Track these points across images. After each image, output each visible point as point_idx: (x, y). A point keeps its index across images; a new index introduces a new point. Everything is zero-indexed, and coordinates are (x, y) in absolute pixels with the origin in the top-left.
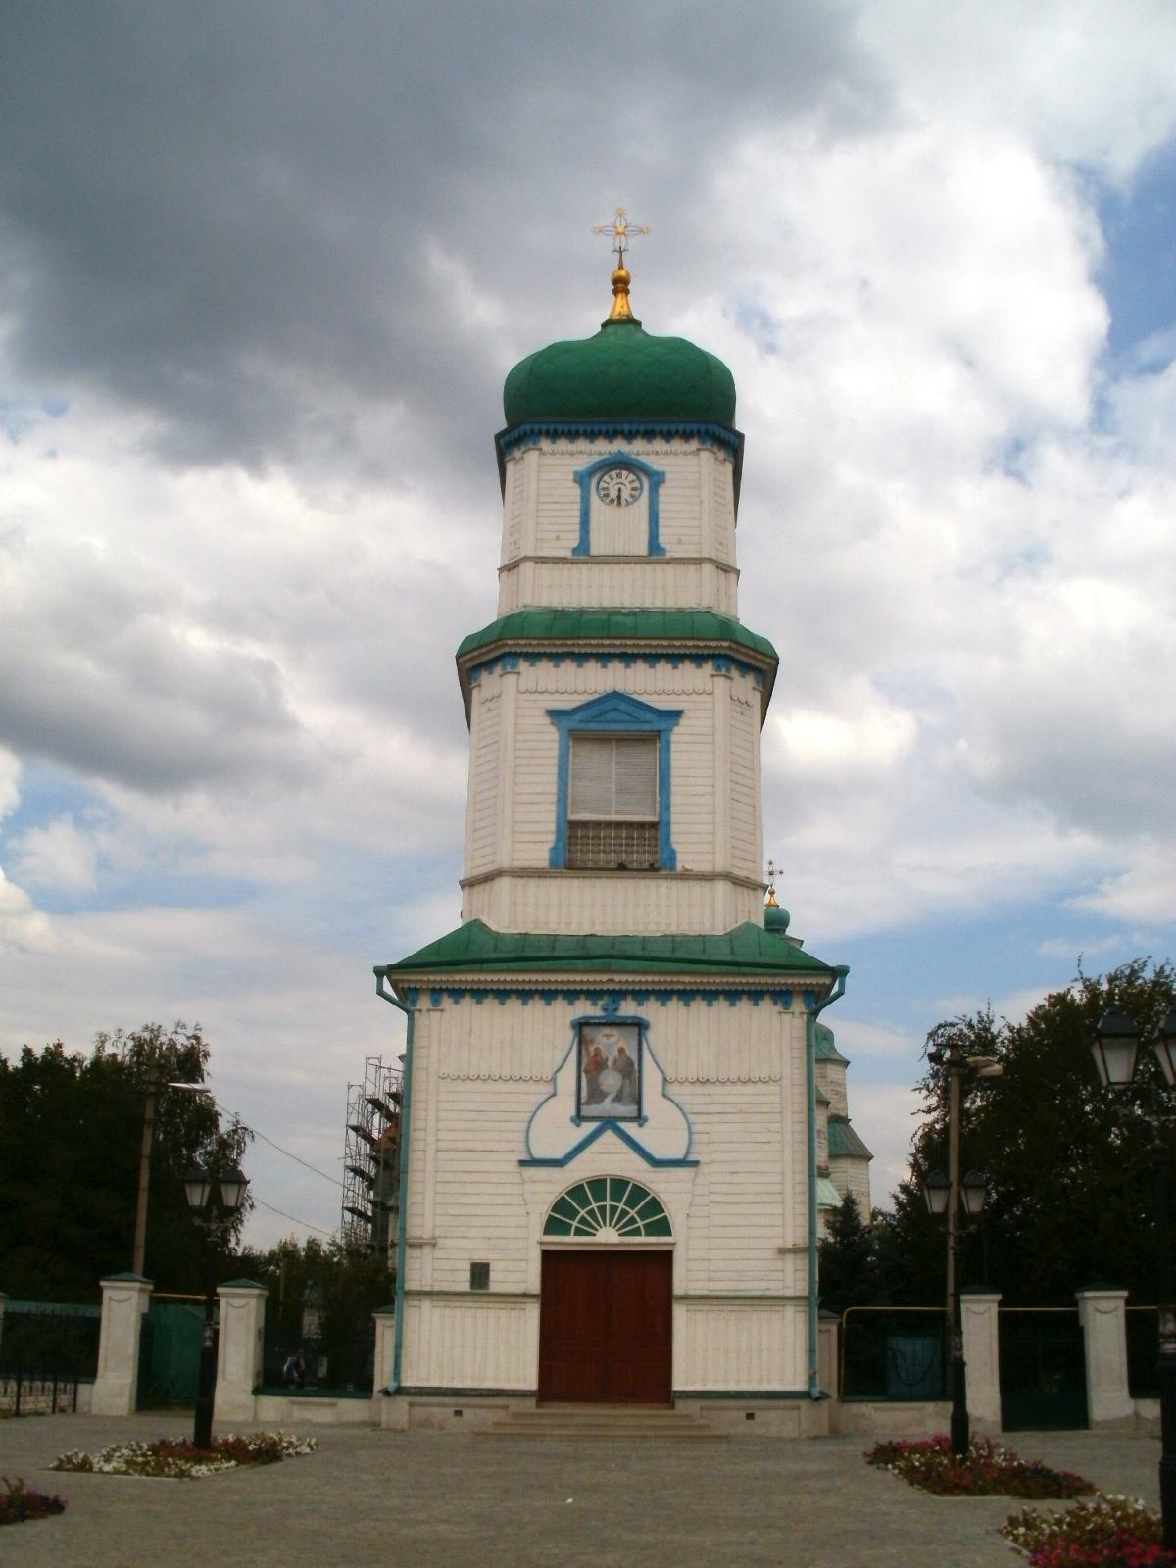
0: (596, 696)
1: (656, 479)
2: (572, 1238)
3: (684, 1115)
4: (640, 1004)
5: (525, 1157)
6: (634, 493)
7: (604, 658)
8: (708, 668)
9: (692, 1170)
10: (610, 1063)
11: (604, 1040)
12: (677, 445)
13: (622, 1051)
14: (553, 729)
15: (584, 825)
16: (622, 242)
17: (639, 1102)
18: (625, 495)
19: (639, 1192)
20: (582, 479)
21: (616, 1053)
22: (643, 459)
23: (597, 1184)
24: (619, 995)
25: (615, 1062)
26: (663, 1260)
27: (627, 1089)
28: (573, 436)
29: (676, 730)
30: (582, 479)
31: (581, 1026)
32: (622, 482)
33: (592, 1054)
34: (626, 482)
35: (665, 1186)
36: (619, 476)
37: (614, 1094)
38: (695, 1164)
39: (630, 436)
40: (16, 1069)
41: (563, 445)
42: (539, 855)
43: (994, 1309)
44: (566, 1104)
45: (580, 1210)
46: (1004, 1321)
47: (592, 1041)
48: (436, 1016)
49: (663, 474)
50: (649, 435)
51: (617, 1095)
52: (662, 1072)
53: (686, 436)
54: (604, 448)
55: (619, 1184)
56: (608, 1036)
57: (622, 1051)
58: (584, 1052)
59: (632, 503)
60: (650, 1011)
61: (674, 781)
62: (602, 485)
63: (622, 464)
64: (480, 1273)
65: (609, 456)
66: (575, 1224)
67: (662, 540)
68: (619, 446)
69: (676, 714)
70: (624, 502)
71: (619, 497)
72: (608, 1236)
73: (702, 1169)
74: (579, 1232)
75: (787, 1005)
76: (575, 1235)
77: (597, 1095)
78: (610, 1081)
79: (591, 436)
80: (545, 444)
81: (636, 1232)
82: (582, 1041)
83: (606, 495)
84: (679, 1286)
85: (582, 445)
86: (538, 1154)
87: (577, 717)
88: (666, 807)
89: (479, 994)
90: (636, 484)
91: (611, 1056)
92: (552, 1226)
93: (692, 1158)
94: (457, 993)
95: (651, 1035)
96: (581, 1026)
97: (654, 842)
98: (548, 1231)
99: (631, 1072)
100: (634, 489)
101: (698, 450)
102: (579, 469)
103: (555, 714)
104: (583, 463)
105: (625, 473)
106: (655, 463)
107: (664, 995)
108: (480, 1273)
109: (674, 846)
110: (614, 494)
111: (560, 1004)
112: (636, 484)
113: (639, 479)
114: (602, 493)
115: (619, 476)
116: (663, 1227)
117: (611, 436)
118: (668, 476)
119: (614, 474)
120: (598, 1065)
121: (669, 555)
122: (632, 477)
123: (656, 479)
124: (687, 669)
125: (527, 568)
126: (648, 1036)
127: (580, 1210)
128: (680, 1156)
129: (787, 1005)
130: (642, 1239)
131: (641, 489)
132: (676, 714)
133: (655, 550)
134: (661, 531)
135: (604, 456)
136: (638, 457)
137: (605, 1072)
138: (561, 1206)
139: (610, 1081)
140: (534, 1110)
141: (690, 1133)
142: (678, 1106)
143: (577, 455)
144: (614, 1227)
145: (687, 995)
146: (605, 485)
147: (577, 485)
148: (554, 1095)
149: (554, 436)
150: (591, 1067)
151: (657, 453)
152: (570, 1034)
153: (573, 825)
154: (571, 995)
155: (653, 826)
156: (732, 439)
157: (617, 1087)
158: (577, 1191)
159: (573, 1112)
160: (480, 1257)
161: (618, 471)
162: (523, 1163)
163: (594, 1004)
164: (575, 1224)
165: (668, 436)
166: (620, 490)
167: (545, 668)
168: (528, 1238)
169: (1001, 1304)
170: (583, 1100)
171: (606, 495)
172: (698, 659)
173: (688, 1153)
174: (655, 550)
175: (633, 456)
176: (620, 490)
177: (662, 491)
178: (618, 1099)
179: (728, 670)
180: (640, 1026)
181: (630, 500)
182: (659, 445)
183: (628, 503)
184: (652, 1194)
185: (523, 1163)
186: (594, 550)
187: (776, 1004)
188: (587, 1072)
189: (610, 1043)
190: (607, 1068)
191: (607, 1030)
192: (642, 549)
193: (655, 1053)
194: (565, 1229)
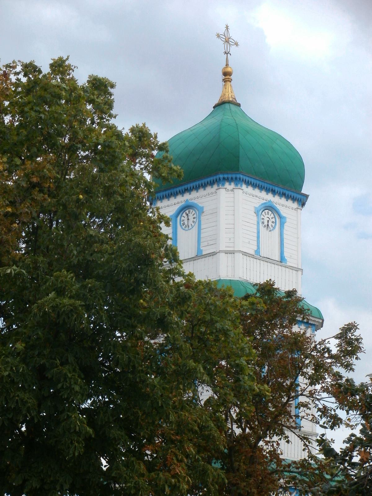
6: (273, 225)
12: (290, 203)
18: (270, 223)
22: (279, 207)
32: (268, 216)
41: (250, 190)
49: (285, 218)
50: (282, 195)
53: (294, 199)
59: (273, 230)
63: (270, 208)
65: (266, 202)
67: (286, 254)
68: (270, 197)
71: (268, 225)
79: (261, 188)
80: (244, 186)
85: (257, 192)
100: (273, 222)
101: (298, 208)
105: (270, 212)
106: (283, 211)
110: (266, 223)
112: (274, 220)
117: (268, 190)
118: (288, 220)
119: (266, 211)
121: (289, 264)
122: (272, 216)
131: (275, 223)
133: (282, 259)
134: (285, 250)
136: (275, 205)
149: (248, 183)
151: (283, 206)
161: (268, 211)
165: (288, 197)
171: (263, 223)
175: (274, 204)
181: (271, 228)
182: (283, 201)
186: (263, 253)
192: (277, 258)
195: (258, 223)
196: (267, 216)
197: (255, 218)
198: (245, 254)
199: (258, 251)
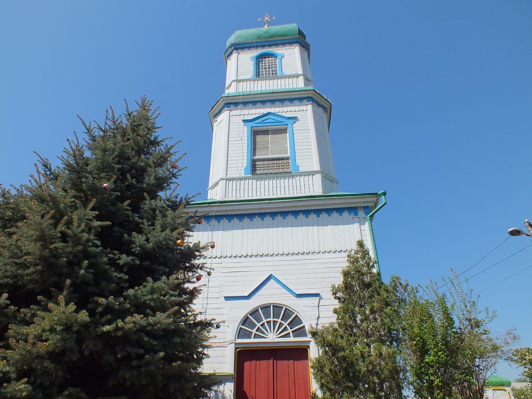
0: (261, 115)
2: (252, 340)
19: (288, 313)
23: (265, 308)
40: (76, 306)
55: (277, 308)
74: (256, 336)
75: (356, 214)
76: (254, 338)
81: (287, 335)
92: (241, 333)
103: (245, 121)
129: (356, 214)
130: (292, 339)
138: (245, 321)
158: (254, 313)
164: (254, 331)
184: (296, 313)
187: (350, 214)
194: (248, 335)
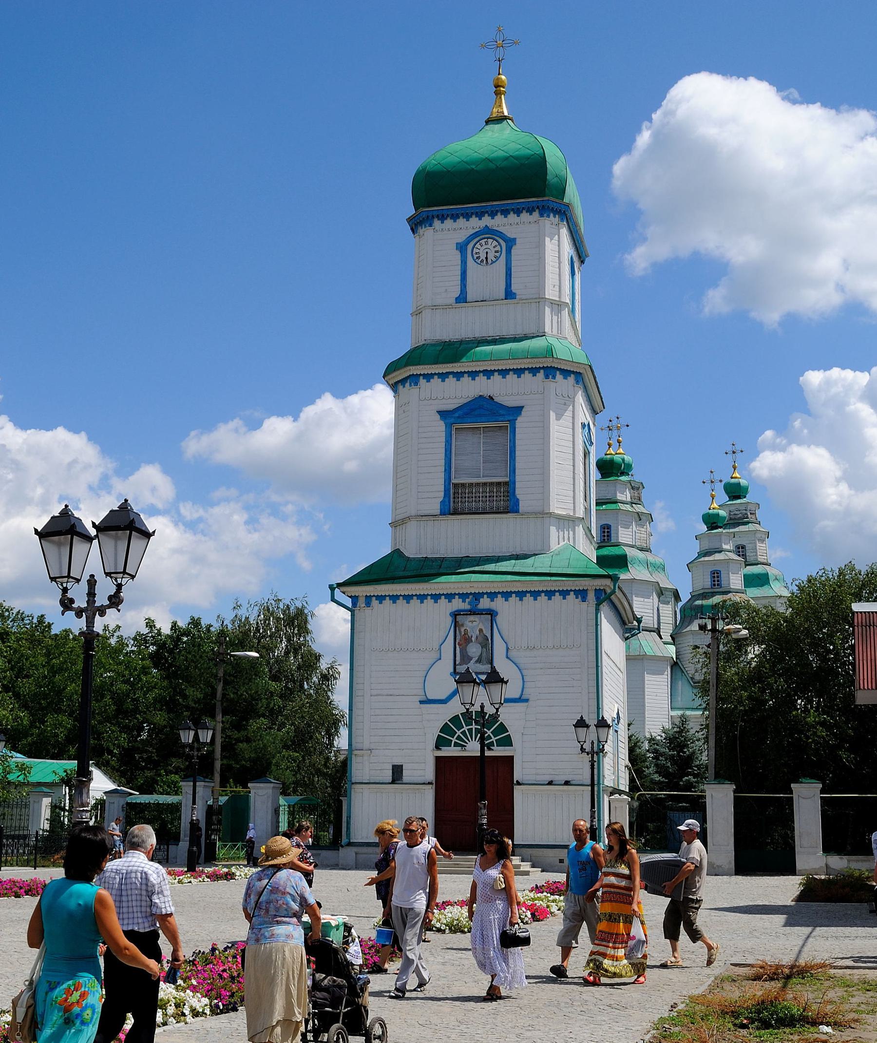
1: (510, 243)
3: (520, 670)
4: (492, 600)
5: (424, 698)
6: (496, 254)
7: (473, 374)
8: (541, 375)
9: (526, 704)
10: (473, 639)
11: (470, 624)
12: (525, 216)
13: (481, 631)
14: (442, 423)
15: (463, 485)
16: (500, 53)
17: (491, 663)
18: (491, 257)
20: (462, 248)
21: (478, 632)
22: (500, 229)
24: (477, 596)
25: (477, 637)
26: (509, 761)
27: (484, 655)
28: (455, 217)
29: (520, 419)
30: (462, 248)
31: (455, 615)
32: (489, 247)
33: (463, 633)
34: (491, 248)
35: (509, 716)
36: (486, 243)
37: (477, 658)
38: (527, 700)
39: (493, 215)
41: (449, 222)
42: (435, 507)
43: (731, 795)
44: (446, 665)
45: (457, 731)
46: (737, 802)
47: (462, 625)
48: (368, 611)
50: (505, 213)
51: (478, 658)
52: (506, 643)
53: (530, 211)
54: (475, 224)
56: (472, 622)
57: (481, 631)
58: (457, 630)
59: (495, 261)
60: (499, 604)
61: (517, 453)
62: (475, 250)
63: (488, 233)
64: (397, 772)
66: (454, 740)
67: (514, 288)
68: (487, 221)
69: (519, 410)
70: (489, 261)
71: (487, 258)
72: (473, 748)
73: (530, 703)
74: (456, 745)
76: (454, 746)
77: (466, 658)
78: (474, 650)
79: (467, 216)
80: (437, 223)
82: (456, 625)
83: (478, 258)
84: (517, 776)
85: (461, 221)
86: (430, 697)
87: (457, 415)
88: (513, 471)
89: (394, 598)
90: (498, 248)
91: (474, 634)
92: (440, 743)
93: (524, 697)
94: (381, 598)
95: (499, 619)
96: (455, 615)
97: (506, 494)
98: (438, 747)
99: (487, 644)
100: (496, 252)
102: (460, 241)
104: (462, 237)
105: (490, 241)
106: (510, 233)
107: (507, 595)
108: (397, 772)
109: (518, 497)
110: (483, 257)
111: (443, 601)
112: (498, 248)
113: (499, 244)
114: (475, 256)
115: (486, 243)
116: (507, 742)
117: (480, 215)
118: (518, 241)
119: (483, 242)
120: (467, 640)
122: (495, 243)
123: (510, 243)
124: (527, 375)
125: (427, 314)
126: (497, 620)
127: (457, 731)
128: (517, 696)
131: (501, 251)
132: (519, 410)
133: (509, 294)
135: (477, 230)
137: (471, 644)
138: (445, 729)
139: (474, 650)
140: (428, 669)
141: (524, 682)
142: (515, 664)
143: (458, 231)
144: (475, 740)
145: (521, 595)
146: (478, 251)
147: (458, 253)
148: (440, 659)
149: (442, 218)
150: (462, 641)
152: (449, 620)
153: (456, 486)
154: (450, 597)
155: (506, 483)
156: (563, 208)
157: (479, 654)
158: (455, 720)
159: (452, 670)
160: (397, 762)
162: (421, 702)
163: (464, 601)
165: (518, 212)
166: (487, 253)
167: (436, 381)
168: (425, 749)
169: (735, 791)
170: (457, 663)
172: (534, 371)
173: (522, 694)
174: (509, 294)
176: (487, 253)
177: (514, 251)
178: (479, 661)
179: (554, 377)
180: (492, 614)
181: (494, 259)
182: (512, 217)
183: (493, 262)
185: (421, 702)
186: (469, 298)
188: (459, 644)
189: (474, 625)
190: (472, 641)
191: (472, 618)
192: (503, 295)
193: (501, 631)
194: (448, 743)
195: (464, 262)
196: (485, 247)
197: (457, 256)
198: (434, 307)
199: (462, 298)
